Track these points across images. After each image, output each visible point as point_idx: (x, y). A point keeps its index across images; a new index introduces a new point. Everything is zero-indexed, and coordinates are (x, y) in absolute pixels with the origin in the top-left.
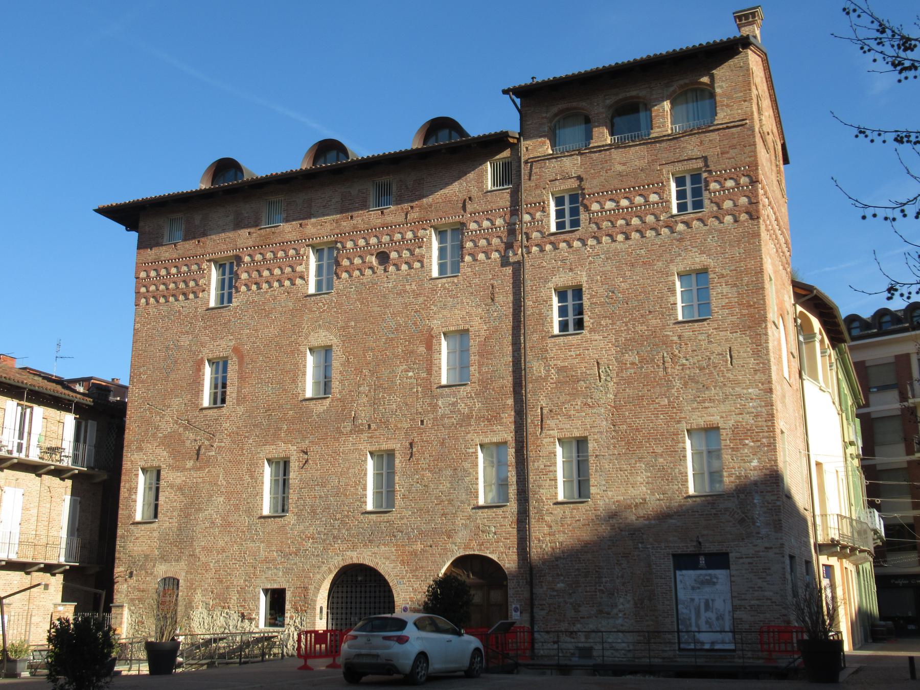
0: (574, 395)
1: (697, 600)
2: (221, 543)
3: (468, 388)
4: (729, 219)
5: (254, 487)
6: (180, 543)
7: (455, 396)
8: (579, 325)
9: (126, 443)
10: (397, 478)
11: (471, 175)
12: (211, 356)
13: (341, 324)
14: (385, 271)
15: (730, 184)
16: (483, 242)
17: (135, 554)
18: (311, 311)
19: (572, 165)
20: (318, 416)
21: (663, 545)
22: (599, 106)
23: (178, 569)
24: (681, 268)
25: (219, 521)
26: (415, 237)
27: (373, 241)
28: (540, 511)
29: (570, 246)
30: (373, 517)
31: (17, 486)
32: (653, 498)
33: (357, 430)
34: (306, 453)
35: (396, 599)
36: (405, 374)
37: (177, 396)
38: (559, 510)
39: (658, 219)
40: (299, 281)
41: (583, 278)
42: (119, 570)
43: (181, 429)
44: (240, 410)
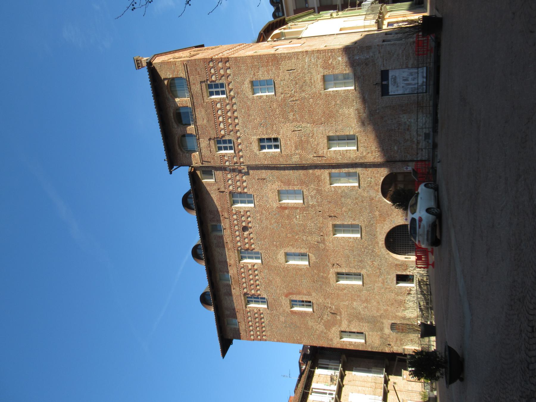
0: (308, 142)
1: (403, 85)
2: (375, 303)
3: (305, 190)
4: (228, 71)
5: (349, 288)
6: (375, 322)
7: (308, 197)
8: (276, 140)
9: (329, 346)
10: (345, 223)
11: (208, 189)
12: (289, 307)
13: (275, 248)
14: (251, 228)
15: (212, 71)
16: (238, 183)
17: (380, 343)
18: (269, 262)
19: (204, 143)
20: (317, 259)
21: (377, 101)
22: (177, 130)
23: (387, 323)
24: (250, 93)
25: (365, 304)
26: (236, 214)
27: (237, 233)
28: (361, 158)
29: (240, 144)
30: (363, 234)
31: (348, 395)
32: (355, 106)
33: (323, 241)
34: (334, 265)
35: (401, 224)
36: (298, 219)
37: (307, 323)
38: (361, 149)
39: (228, 104)
40: (255, 267)
41: (255, 138)
42: (387, 350)
43: (323, 321)
44: (314, 294)
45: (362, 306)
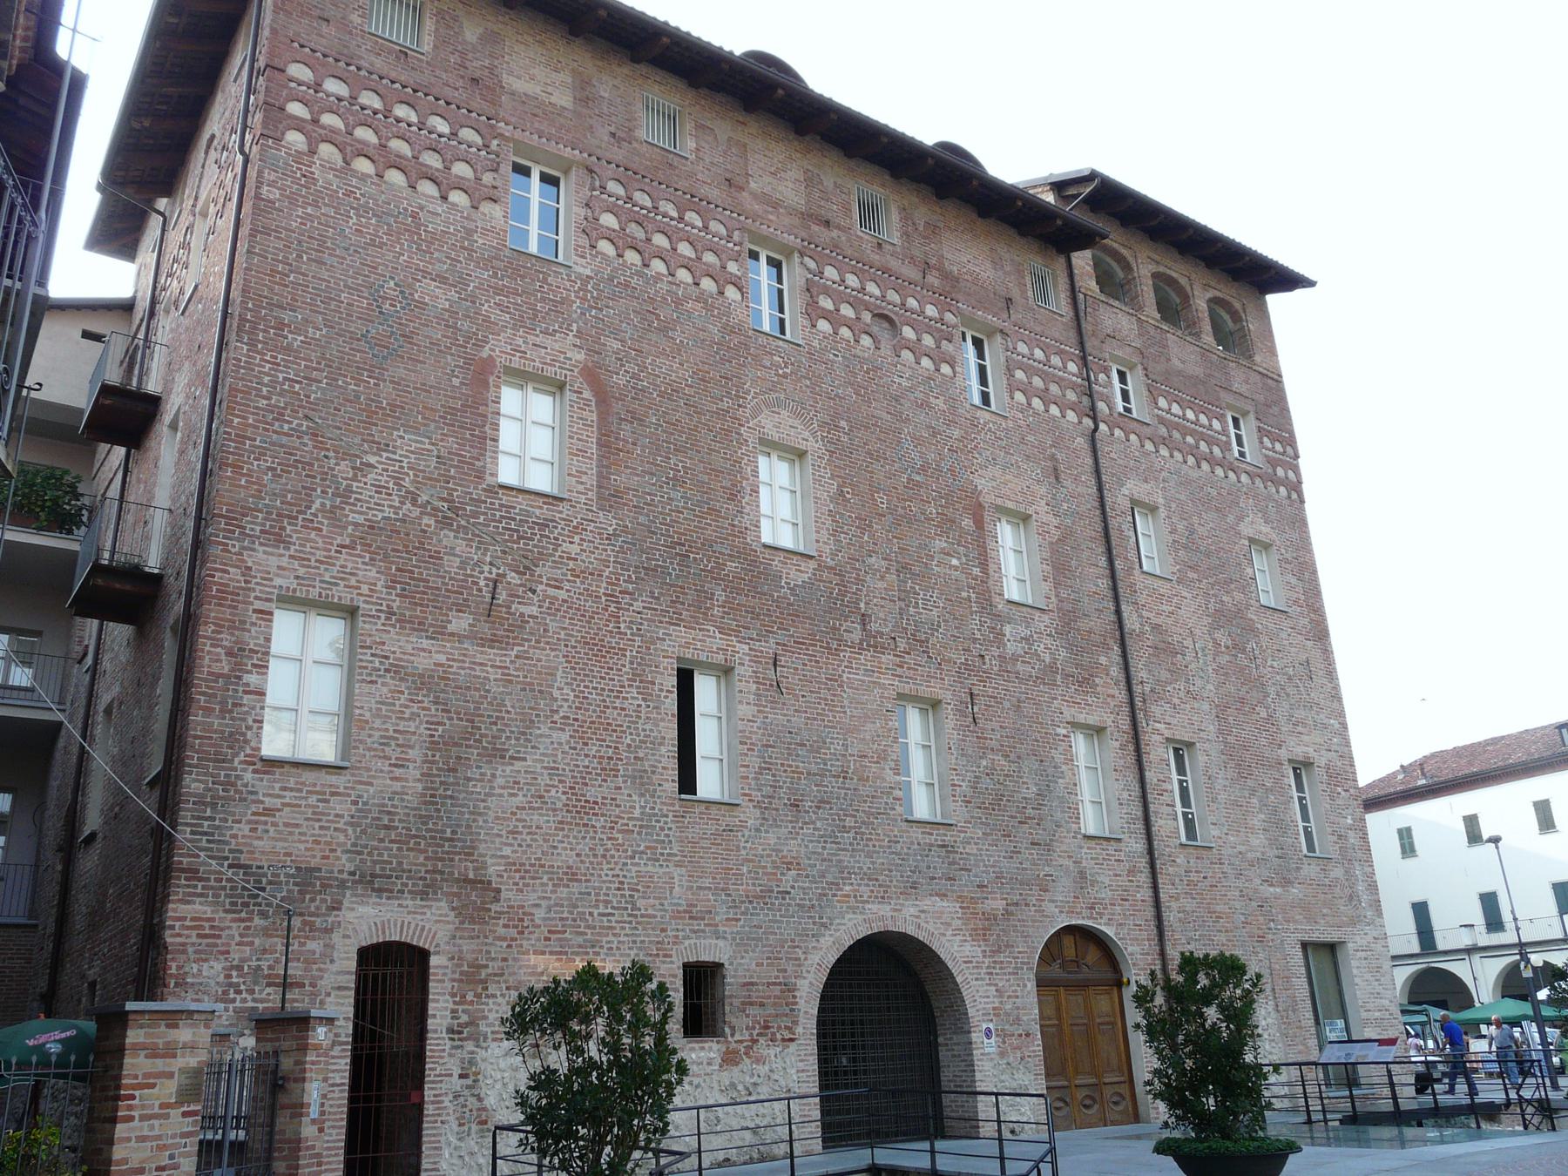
25: (557, 796)
33: (872, 643)
37: (415, 429)
40: (732, 293)
44: (609, 522)
45: (544, 780)
